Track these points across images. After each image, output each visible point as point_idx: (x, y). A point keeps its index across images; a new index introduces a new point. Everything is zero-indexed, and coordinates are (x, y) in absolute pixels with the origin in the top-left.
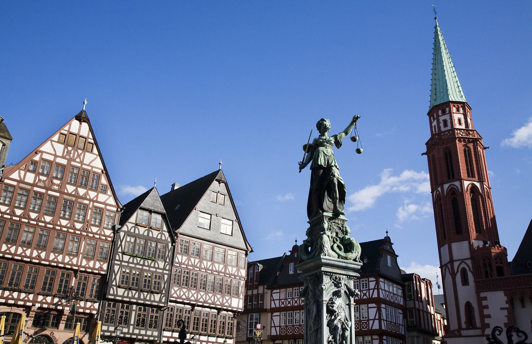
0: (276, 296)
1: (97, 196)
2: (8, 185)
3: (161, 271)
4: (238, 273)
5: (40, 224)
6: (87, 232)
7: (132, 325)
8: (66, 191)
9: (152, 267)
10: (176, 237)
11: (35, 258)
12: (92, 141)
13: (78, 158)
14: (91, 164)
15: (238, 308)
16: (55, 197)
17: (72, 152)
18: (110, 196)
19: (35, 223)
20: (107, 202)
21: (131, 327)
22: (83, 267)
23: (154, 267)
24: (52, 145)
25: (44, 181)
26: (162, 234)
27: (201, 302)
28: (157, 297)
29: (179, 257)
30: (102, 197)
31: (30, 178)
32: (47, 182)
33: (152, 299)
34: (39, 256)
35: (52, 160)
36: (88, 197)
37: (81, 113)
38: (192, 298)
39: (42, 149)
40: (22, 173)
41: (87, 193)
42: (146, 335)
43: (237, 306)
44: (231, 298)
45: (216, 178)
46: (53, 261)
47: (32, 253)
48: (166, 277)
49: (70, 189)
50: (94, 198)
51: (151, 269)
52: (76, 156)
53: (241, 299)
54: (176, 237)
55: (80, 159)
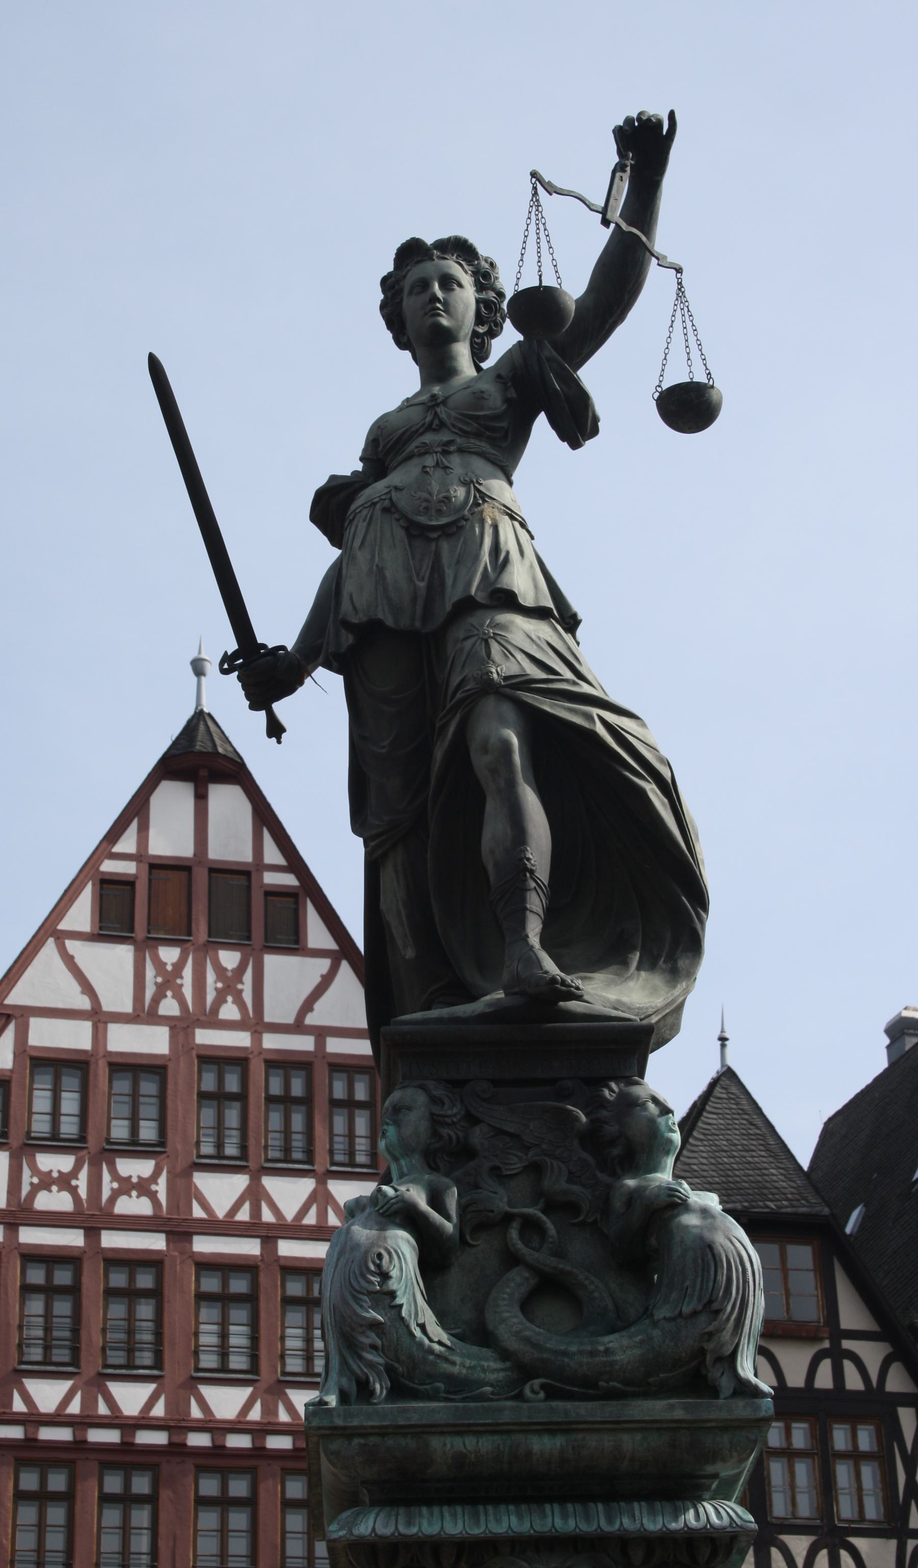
8: (198, 1212)
13: (230, 999)
14: (310, 1020)
24: (69, 961)
26: (838, 1356)
35: (85, 1044)
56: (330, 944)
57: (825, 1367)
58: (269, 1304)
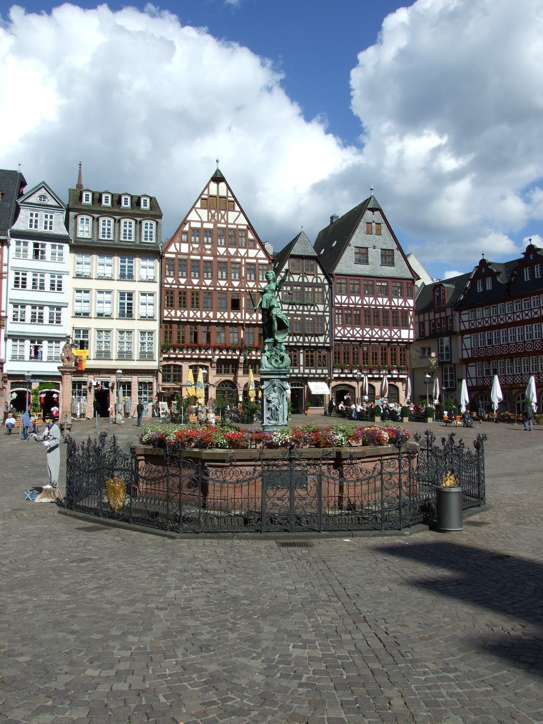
0: (465, 318)
1: (247, 252)
2: (168, 259)
3: (321, 314)
4: (405, 304)
5: (203, 288)
6: (245, 288)
7: (302, 366)
8: (218, 254)
9: (312, 311)
10: (331, 279)
11: (205, 319)
12: (232, 199)
14: (236, 223)
15: (409, 339)
16: (210, 262)
17: (216, 215)
18: (259, 250)
19: (198, 288)
20: (258, 256)
21: (302, 368)
22: (248, 320)
23: (314, 311)
24: (197, 212)
25: (197, 249)
26: (317, 277)
27: (367, 338)
28: (322, 339)
29: (339, 297)
30: (252, 253)
31: (185, 248)
32: (200, 249)
33: (317, 341)
34: (208, 316)
36: (239, 255)
37: (216, 173)
38: (358, 335)
39: (188, 219)
40: (178, 245)
41: (237, 252)
42: (316, 374)
43: (407, 337)
44: (400, 330)
45: (368, 207)
46: (220, 319)
47: (201, 315)
48: (327, 319)
49: (222, 251)
50: (245, 254)
51: (312, 313)
52: (220, 218)
53: (412, 329)
54: (331, 279)
55: (224, 219)
56: (239, 210)
57: (315, 279)
58: (229, 269)
